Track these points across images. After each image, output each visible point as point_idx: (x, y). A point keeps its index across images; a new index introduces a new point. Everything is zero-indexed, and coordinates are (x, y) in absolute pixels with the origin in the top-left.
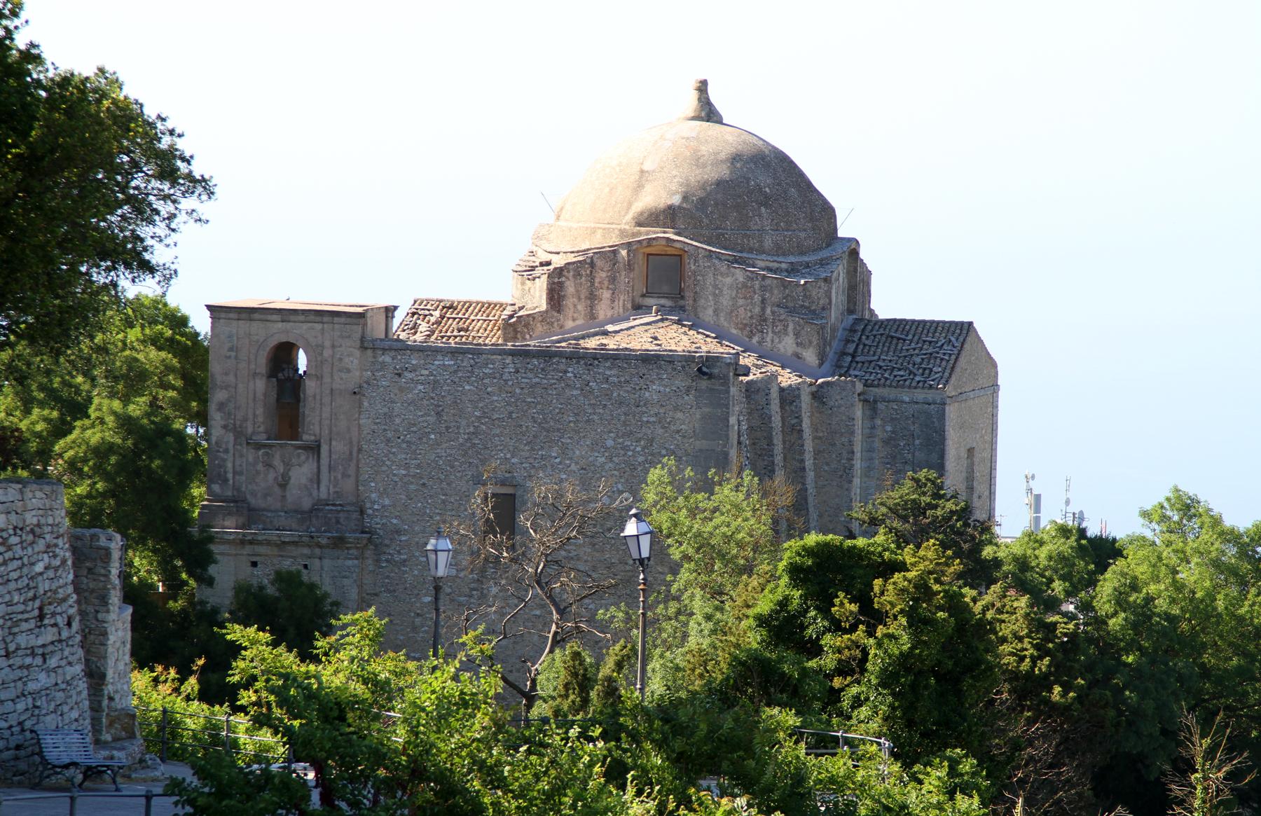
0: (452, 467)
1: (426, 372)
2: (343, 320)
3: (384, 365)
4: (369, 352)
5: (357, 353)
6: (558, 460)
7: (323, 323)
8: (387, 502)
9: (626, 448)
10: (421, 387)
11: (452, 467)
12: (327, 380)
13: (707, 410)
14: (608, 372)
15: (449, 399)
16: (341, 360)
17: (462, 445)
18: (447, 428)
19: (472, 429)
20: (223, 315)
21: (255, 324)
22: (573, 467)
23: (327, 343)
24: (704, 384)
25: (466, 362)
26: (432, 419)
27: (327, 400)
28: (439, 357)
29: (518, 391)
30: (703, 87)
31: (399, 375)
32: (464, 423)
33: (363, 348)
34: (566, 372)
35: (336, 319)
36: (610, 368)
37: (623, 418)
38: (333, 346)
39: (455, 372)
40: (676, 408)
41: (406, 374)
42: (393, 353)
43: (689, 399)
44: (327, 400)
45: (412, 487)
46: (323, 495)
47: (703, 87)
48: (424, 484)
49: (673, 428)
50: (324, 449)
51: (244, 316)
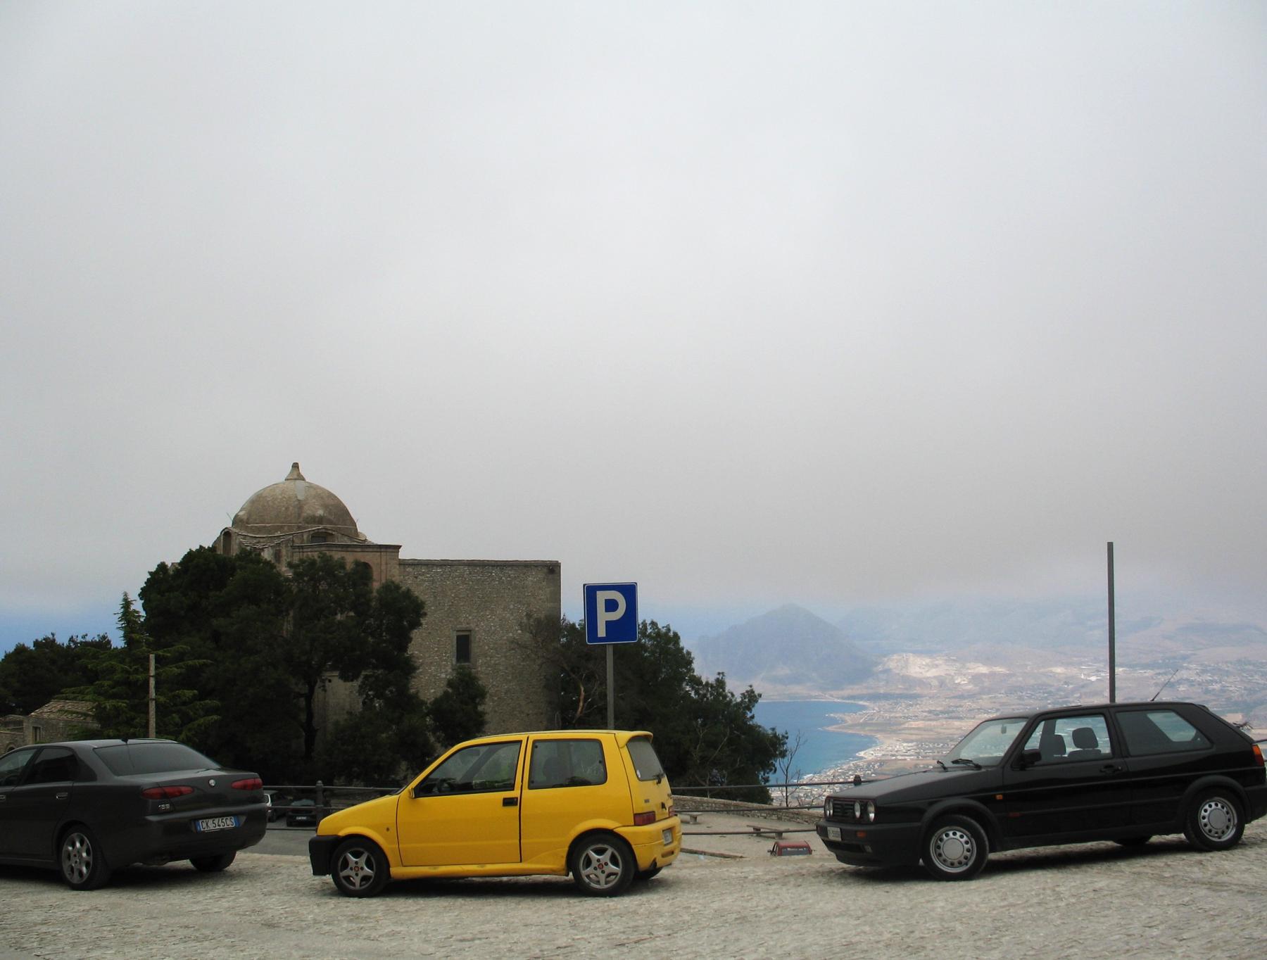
0: (442, 623)
1: (428, 575)
2: (390, 550)
3: (409, 573)
4: (402, 567)
5: (398, 567)
6: (489, 616)
7: (381, 552)
9: (519, 609)
10: (427, 583)
11: (442, 623)
13: (552, 588)
14: (510, 572)
15: (440, 589)
16: (390, 571)
17: (446, 611)
18: (439, 603)
19: (450, 604)
20: (334, 549)
21: (348, 553)
22: (496, 619)
23: (383, 562)
24: (550, 576)
28: (435, 568)
29: (471, 583)
30: (296, 466)
31: (416, 577)
32: (447, 600)
33: (400, 564)
34: (492, 573)
35: (389, 550)
36: (511, 571)
37: (517, 594)
38: (386, 564)
39: (442, 575)
40: (540, 588)
41: (420, 577)
42: (413, 567)
43: (544, 583)
45: (424, 634)
47: (296, 466)
48: (430, 633)
49: (538, 598)
51: (344, 549)
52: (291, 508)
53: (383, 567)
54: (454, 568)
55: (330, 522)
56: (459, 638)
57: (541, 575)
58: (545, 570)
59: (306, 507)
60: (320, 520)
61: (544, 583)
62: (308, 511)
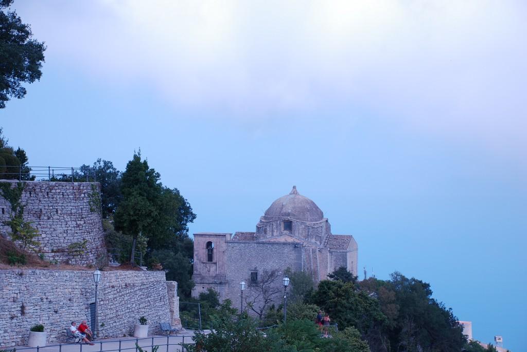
5: (224, 243)
8: (231, 274)
12: (218, 249)
24: (296, 249)
25: (247, 245)
26: (240, 257)
27: (218, 253)
30: (294, 187)
40: (290, 254)
43: (293, 252)
44: (218, 253)
46: (217, 273)
47: (294, 187)
50: (218, 264)
52: (278, 209)
53: (218, 243)
54: (250, 244)
55: (294, 215)
56: (252, 273)
57: (291, 248)
58: (294, 246)
59: (284, 208)
60: (289, 214)
61: (293, 252)
62: (284, 211)
